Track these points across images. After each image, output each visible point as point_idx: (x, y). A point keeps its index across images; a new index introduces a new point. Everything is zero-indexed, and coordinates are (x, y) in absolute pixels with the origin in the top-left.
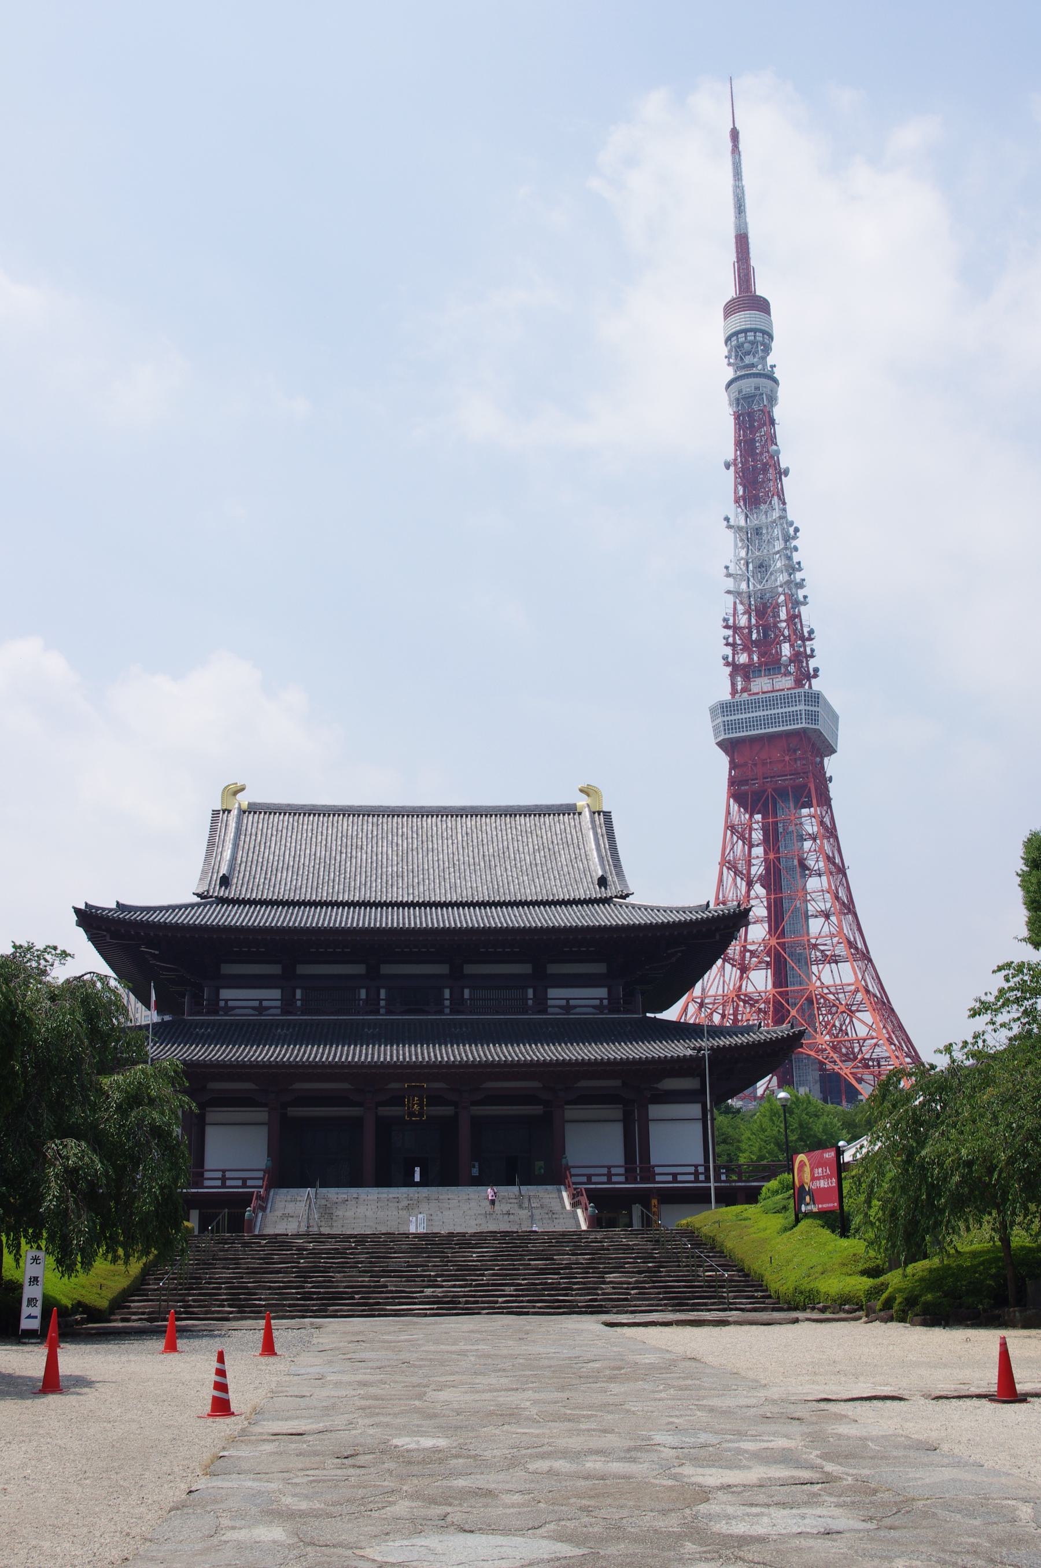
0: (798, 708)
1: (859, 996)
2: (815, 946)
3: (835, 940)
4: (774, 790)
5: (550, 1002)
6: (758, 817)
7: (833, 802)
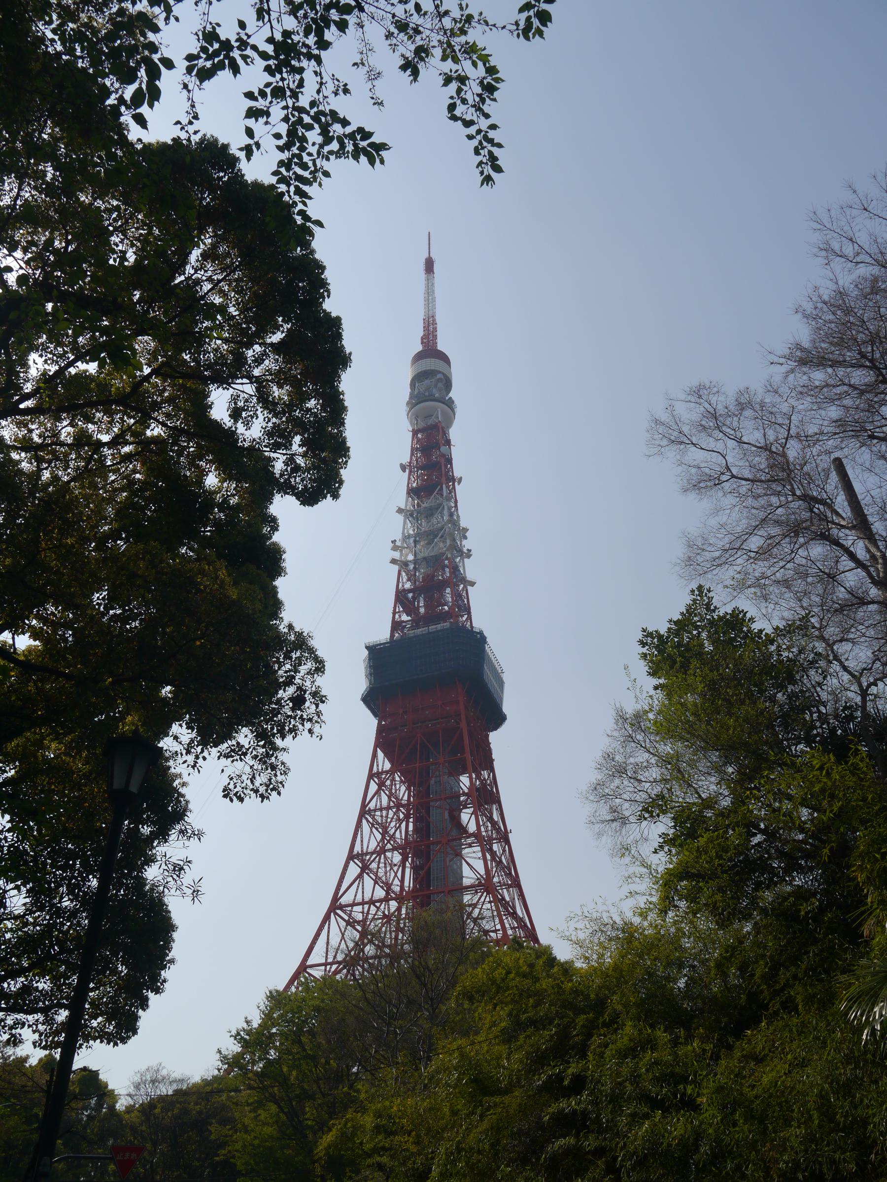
7: (496, 765)
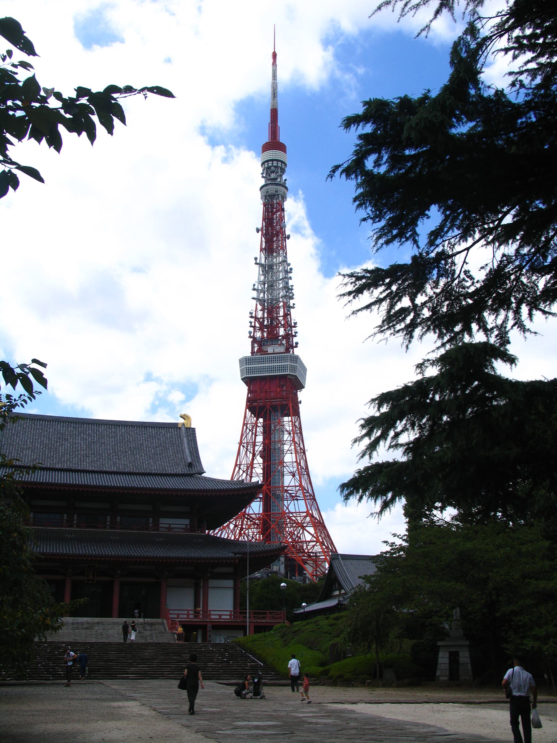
0: (286, 363)
1: (308, 519)
2: (287, 491)
3: (297, 488)
4: (270, 406)
5: (161, 525)
6: (261, 420)
